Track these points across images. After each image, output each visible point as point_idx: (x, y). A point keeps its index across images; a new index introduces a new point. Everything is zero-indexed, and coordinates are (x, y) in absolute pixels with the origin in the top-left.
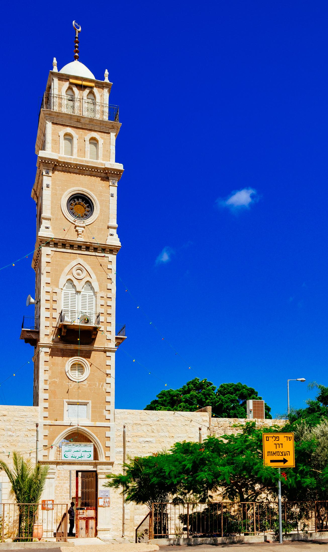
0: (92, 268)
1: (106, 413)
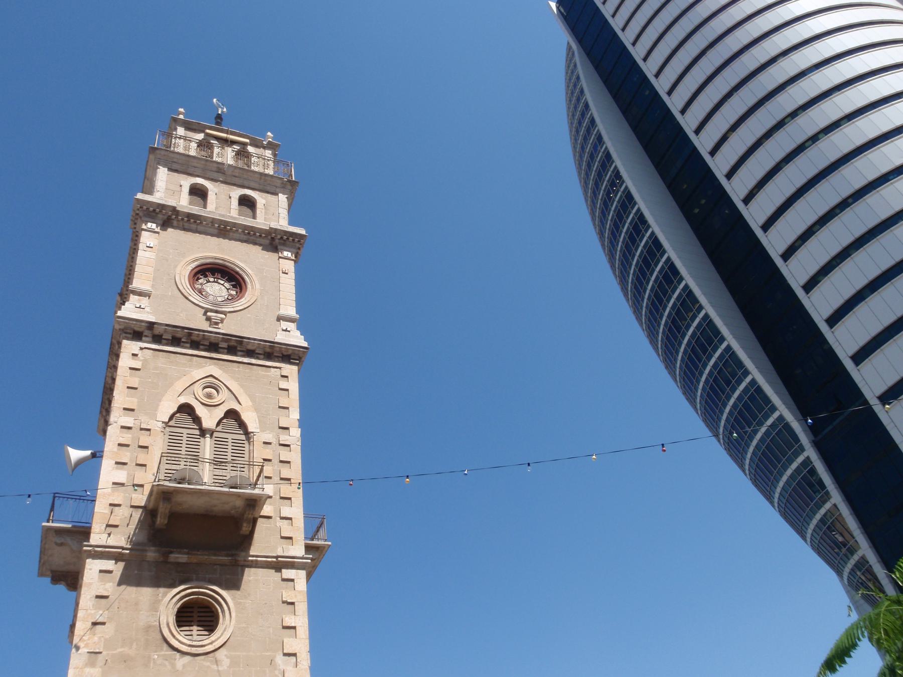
0: (242, 386)
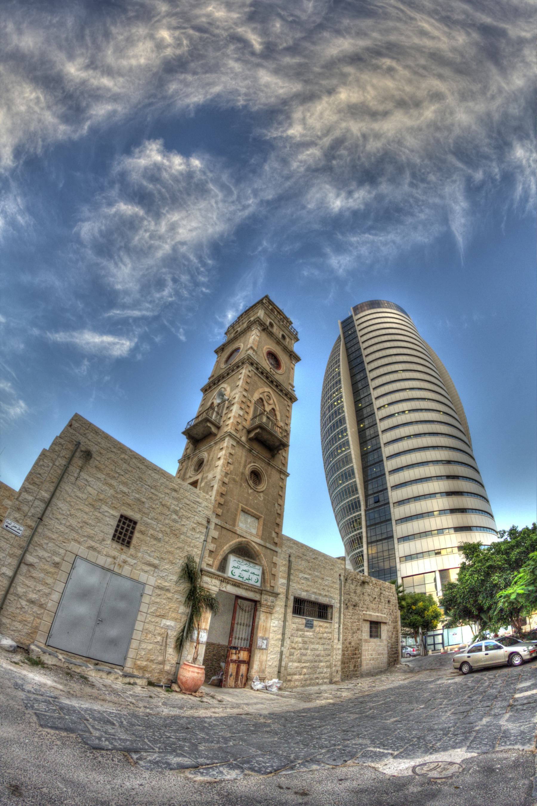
1: (274, 535)
